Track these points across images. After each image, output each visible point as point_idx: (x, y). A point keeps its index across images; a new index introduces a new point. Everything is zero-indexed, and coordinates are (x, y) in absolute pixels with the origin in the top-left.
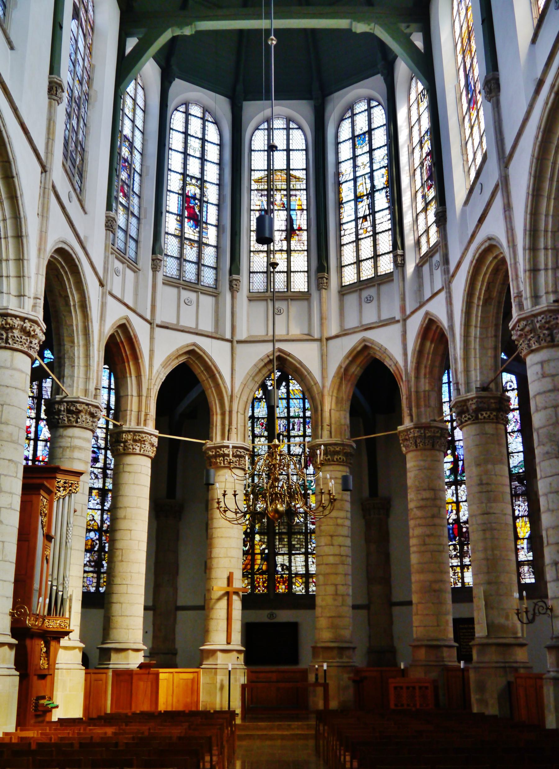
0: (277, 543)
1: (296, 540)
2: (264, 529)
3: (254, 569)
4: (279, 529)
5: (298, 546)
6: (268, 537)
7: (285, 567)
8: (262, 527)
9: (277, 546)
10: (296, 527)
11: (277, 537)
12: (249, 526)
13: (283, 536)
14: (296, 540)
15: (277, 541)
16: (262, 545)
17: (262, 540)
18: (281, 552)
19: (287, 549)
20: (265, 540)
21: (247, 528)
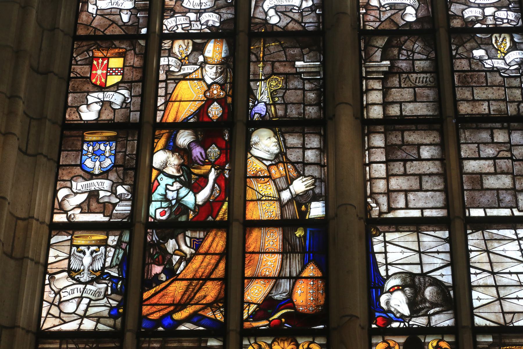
0: (380, 170)
1: (490, 151)
2: (304, 103)
3: (242, 303)
4: (385, 104)
5: (506, 181)
6: (324, 139)
7: (429, 292)
8: (292, 96)
9: (381, 186)
10: (480, 93)
11: (378, 141)
12: (216, 91)
13: (412, 137)
14: (490, 151)
15: (379, 155)
16: (290, 181)
17: (293, 156)
18: (401, 214)
19: (439, 199)
20: (311, 156)
21: (209, 101)
